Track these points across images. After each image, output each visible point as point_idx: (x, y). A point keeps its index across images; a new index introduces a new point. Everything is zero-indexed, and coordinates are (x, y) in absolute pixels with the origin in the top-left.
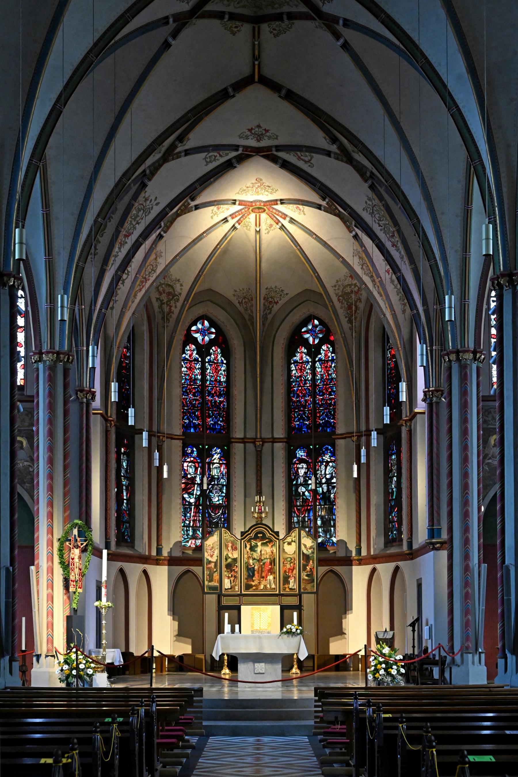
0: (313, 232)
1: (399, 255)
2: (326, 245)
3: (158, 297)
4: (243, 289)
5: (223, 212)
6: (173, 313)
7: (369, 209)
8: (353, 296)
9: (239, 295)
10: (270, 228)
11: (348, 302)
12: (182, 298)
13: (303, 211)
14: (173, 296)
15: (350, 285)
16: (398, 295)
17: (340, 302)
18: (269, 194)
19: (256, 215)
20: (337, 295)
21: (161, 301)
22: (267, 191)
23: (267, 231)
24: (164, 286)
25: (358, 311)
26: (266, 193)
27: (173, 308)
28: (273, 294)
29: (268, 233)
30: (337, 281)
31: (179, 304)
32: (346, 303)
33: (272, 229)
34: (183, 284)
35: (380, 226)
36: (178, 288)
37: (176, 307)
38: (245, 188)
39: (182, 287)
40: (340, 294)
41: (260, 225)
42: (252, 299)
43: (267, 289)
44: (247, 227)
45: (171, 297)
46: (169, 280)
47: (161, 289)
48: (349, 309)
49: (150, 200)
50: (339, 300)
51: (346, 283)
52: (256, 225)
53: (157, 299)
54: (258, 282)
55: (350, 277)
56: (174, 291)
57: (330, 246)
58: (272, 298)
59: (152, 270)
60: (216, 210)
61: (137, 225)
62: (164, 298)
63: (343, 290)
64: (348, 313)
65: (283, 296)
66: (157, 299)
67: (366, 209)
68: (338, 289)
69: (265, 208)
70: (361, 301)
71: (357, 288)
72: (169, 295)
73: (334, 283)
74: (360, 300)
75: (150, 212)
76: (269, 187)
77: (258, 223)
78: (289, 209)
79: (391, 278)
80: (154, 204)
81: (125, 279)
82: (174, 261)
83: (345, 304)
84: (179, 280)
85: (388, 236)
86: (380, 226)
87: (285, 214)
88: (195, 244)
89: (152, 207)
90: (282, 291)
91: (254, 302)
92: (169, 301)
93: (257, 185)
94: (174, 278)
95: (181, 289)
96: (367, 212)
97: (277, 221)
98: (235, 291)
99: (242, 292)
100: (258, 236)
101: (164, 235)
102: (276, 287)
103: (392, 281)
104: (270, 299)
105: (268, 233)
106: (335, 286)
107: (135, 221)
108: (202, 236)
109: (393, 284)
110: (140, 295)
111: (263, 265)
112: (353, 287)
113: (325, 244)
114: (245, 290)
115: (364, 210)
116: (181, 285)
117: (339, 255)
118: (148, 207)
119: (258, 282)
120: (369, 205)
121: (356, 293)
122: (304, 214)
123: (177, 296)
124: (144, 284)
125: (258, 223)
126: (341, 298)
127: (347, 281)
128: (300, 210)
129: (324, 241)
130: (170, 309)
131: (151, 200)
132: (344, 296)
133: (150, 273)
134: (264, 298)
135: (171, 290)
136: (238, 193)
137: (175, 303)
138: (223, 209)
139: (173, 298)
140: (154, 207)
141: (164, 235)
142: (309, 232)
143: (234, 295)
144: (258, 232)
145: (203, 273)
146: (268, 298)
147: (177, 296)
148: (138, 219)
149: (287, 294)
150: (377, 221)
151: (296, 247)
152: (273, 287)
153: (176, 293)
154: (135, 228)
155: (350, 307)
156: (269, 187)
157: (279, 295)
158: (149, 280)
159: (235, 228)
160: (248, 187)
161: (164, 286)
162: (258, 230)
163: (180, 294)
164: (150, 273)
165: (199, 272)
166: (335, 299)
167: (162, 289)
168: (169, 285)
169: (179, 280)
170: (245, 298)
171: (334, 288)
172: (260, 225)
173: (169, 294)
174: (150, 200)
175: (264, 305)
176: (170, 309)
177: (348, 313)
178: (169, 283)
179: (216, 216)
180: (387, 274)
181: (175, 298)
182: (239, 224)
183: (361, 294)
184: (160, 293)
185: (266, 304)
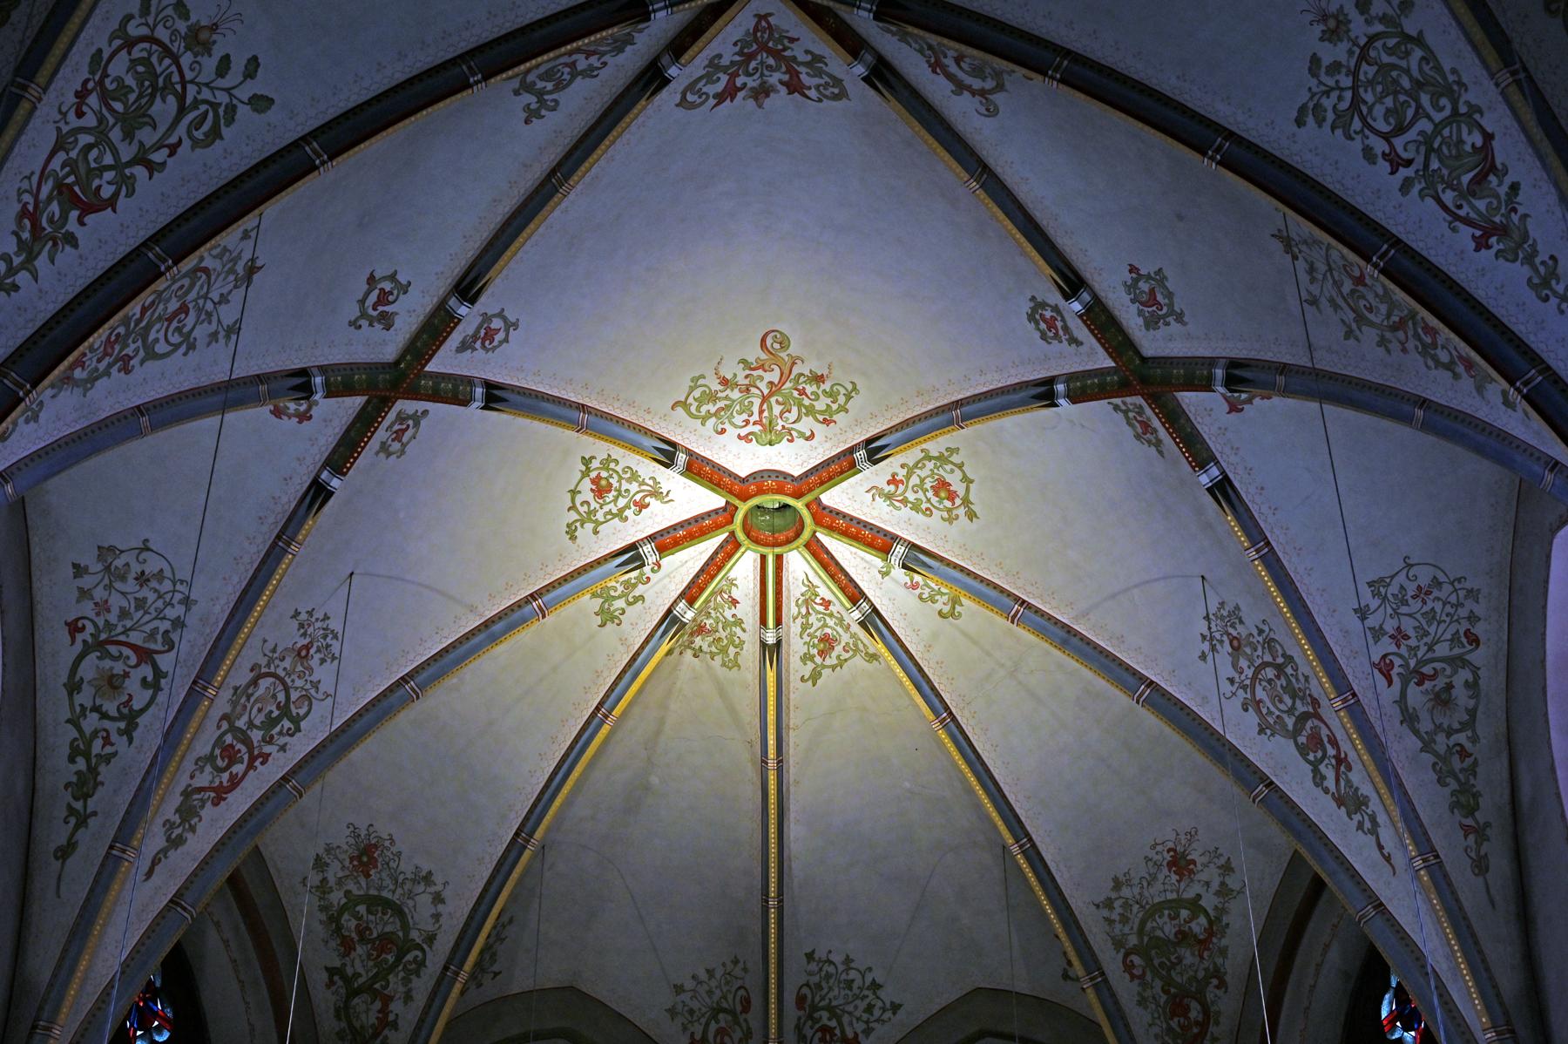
0: (1009, 594)
1: (1526, 271)
2: (1075, 641)
3: (337, 963)
4: (710, 973)
5: (620, 515)
6: (394, 1025)
7: (1327, 103)
8: (1188, 957)
9: (695, 1005)
10: (821, 653)
11: (1168, 983)
12: (436, 958)
13: (966, 502)
14: (397, 949)
15: (1175, 905)
16: (1441, 782)
17: (1133, 977)
18: (820, 430)
19: (763, 558)
20: (1118, 944)
21: (348, 981)
22: (810, 411)
23: (810, 666)
24: (362, 909)
25: (1212, 1029)
26: (806, 425)
27: (396, 1007)
28: (837, 995)
29: (815, 676)
30: (1117, 885)
31: (422, 986)
32: (1158, 984)
33: (828, 662)
34: (447, 894)
35: (1396, 163)
36: (421, 909)
37: (408, 997)
38: (715, 386)
39: (440, 907)
40: (1133, 940)
41: (778, 622)
42: (746, 1004)
43: (810, 957)
44: (724, 651)
45: (390, 958)
46: (388, 881)
47: (349, 923)
48: (1173, 1014)
49: (218, 52)
50: (1129, 967)
51: (1155, 894)
52: (763, 622)
53: (331, 971)
54: (772, 764)
55: (1170, 865)
56: (405, 927)
57: (1089, 642)
58: (831, 1009)
59: (285, 710)
60: (589, 496)
61: (140, 171)
62: (360, 963)
63: (1143, 923)
64: (1170, 1030)
65: (877, 1012)
66: (331, 971)
67: (1318, 107)
68: (1124, 919)
69: (799, 505)
70: (1222, 984)
71: (1203, 920)
72: (382, 950)
73: (1106, 891)
74: (1217, 973)
75: (215, 134)
76: (818, 379)
77: (771, 584)
78: (905, 501)
79: (1402, 701)
80: (244, 93)
81: (143, 711)
82: (393, 698)
83: (1158, 990)
84: (428, 879)
85: (1448, 197)
86: (1396, 163)
87: (886, 533)
88: (494, 639)
89: (231, 110)
90: (875, 986)
91: (754, 1018)
92: (384, 973)
93: (768, 377)
94: (406, 867)
95: (437, 917)
96: (1320, 122)
97: (851, 589)
98: (679, 989)
99: (702, 989)
100: (771, 676)
101: (335, 483)
102: (848, 961)
103: (1409, 718)
104: (825, 1015)
105: (815, 676)
106: (1109, 904)
107: (128, 135)
108: (528, 609)
109: (1416, 733)
110: (215, 823)
111: (794, 830)
112: (1184, 913)
113: (1067, 638)
114: (719, 973)
115: (1300, 122)
116: (438, 899)
117: (1135, 673)
118: (206, 94)
119: (772, 764)
120: (1335, 67)
121: (1203, 944)
122: (972, 515)
123: (419, 947)
124: (238, 769)
125: (771, 584)
126: (1136, 960)
127: (1158, 886)
128: (952, 496)
129: (1064, 626)
130: (384, 1011)
131: (224, 65)
132: (1150, 954)
133: (271, 722)
134: (801, 1001)
135: (392, 926)
136: (684, 404)
137: (406, 981)
138: (622, 502)
139: (399, 959)
140: (243, 111)
141: (335, 483)
142: (994, 594)
143: (672, 1012)
144: (772, 652)
145: (531, 835)
146: (814, 1008)
147: (419, 947)
148: (147, 136)
149: (895, 1008)
150: (1380, 146)
151: (937, 715)
152: (838, 958)
153: (414, 935)
154: (126, 183)
155: (1177, 1007)
156: (818, 379)
157: (862, 1005)
158: (266, 758)
159: (675, 620)
160: (725, 382)
161: (362, 909)
162: (771, 639)
163: (431, 938)
164: (271, 722)
165: (517, 834)
166: (1111, 962)
167: (353, 923)
168: (387, 904)
169: (428, 879)
170: (716, 1011)
171: (1106, 913)
172: (778, 622)
173: (385, 941)
174: (218, 52)
175: (799, 1028)
176: (384, 1011)
177: (1170, 1030)
178: (385, 894)
179: (589, 526)
180: (1381, 680)
181: (409, 957)
182: (691, 602)
183: (1223, 952)
184: (347, 946)
185: (808, 1032)
